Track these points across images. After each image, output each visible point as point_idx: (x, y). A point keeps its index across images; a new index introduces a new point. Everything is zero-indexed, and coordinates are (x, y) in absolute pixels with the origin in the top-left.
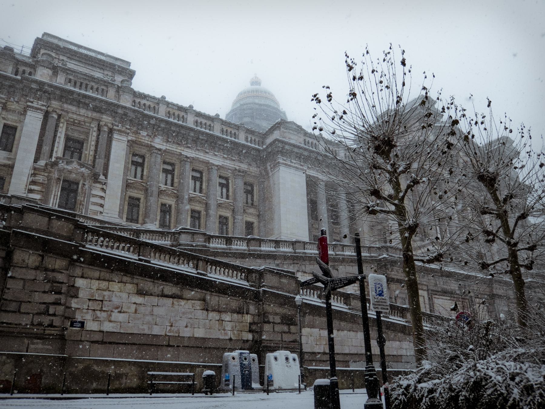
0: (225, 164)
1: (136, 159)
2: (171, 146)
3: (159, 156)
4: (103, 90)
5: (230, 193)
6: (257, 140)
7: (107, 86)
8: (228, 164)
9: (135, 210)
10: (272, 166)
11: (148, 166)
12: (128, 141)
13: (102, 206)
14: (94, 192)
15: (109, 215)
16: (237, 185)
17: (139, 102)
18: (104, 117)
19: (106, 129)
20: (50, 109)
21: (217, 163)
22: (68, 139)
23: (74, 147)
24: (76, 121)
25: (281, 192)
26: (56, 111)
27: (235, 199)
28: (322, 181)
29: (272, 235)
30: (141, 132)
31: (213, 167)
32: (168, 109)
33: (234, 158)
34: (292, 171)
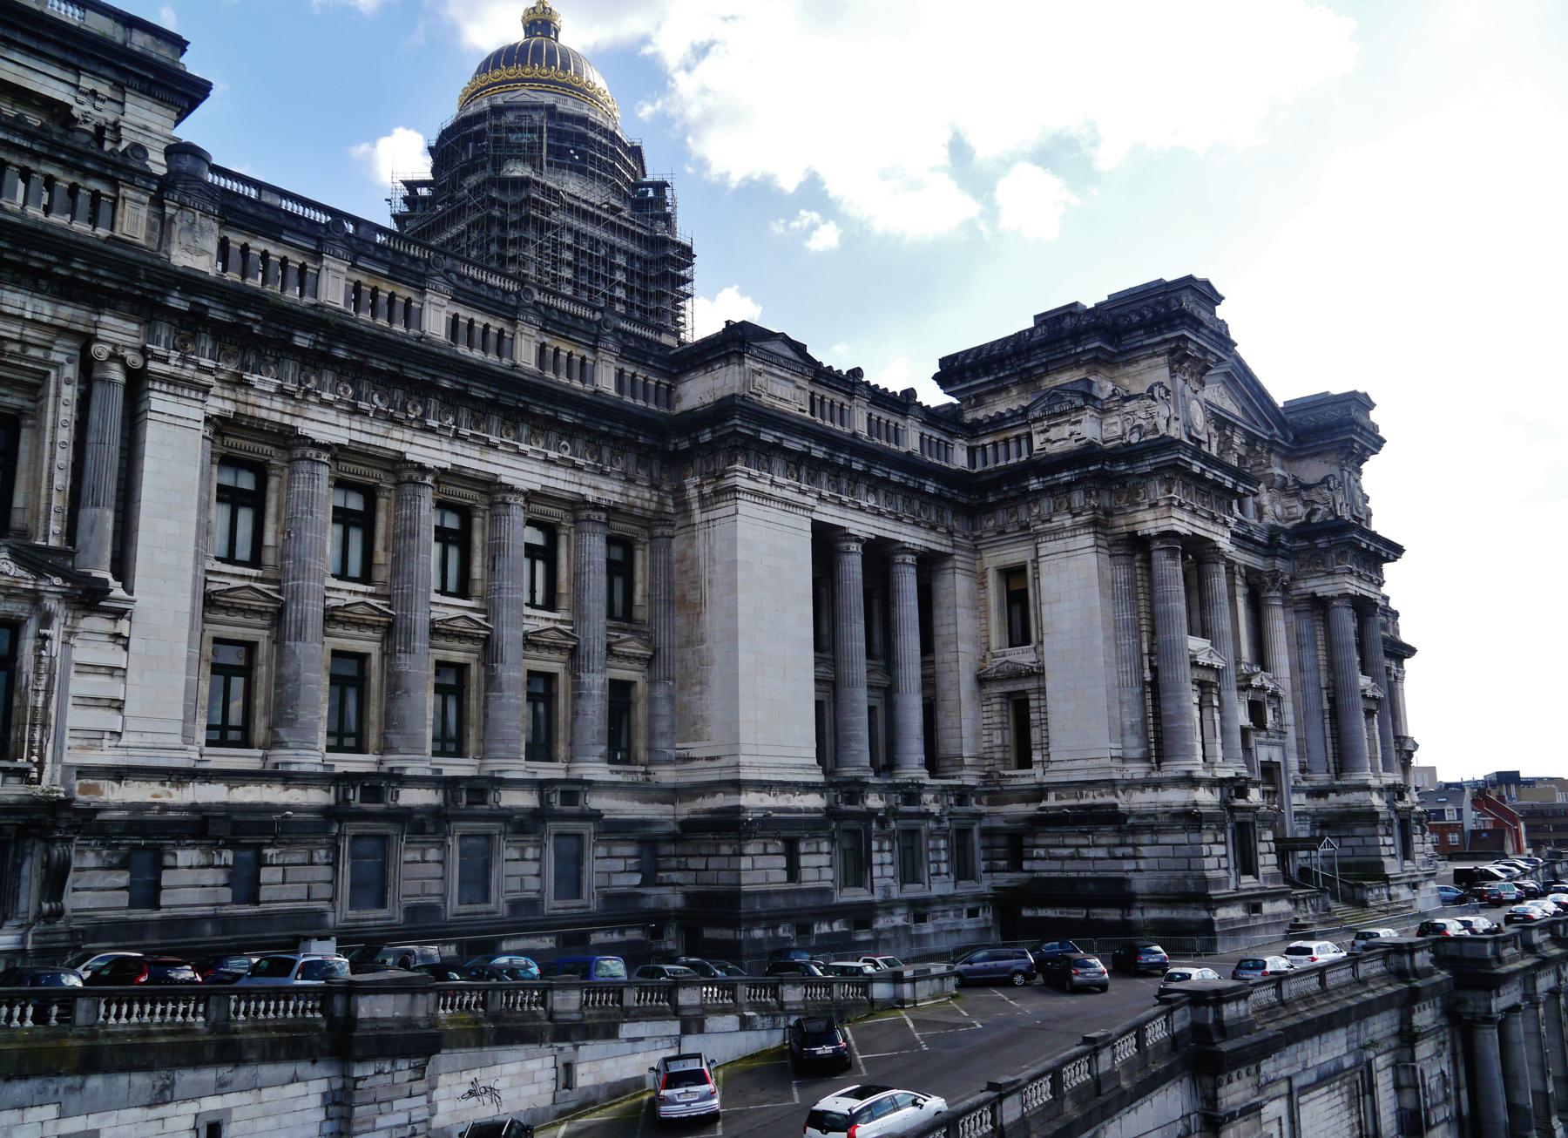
0: (551, 483)
1: (228, 479)
2: (367, 428)
4: (96, 195)
6: (652, 380)
7: (114, 183)
8: (561, 481)
9: (237, 684)
10: (707, 490)
11: (279, 507)
12: (208, 420)
13: (118, 705)
15: (148, 740)
17: (245, 249)
18: (107, 319)
19: (116, 374)
25: (741, 597)
27: (578, 606)
29: (698, 737)
30: (256, 377)
31: (511, 498)
32: (356, 277)
33: (580, 461)
34: (774, 513)
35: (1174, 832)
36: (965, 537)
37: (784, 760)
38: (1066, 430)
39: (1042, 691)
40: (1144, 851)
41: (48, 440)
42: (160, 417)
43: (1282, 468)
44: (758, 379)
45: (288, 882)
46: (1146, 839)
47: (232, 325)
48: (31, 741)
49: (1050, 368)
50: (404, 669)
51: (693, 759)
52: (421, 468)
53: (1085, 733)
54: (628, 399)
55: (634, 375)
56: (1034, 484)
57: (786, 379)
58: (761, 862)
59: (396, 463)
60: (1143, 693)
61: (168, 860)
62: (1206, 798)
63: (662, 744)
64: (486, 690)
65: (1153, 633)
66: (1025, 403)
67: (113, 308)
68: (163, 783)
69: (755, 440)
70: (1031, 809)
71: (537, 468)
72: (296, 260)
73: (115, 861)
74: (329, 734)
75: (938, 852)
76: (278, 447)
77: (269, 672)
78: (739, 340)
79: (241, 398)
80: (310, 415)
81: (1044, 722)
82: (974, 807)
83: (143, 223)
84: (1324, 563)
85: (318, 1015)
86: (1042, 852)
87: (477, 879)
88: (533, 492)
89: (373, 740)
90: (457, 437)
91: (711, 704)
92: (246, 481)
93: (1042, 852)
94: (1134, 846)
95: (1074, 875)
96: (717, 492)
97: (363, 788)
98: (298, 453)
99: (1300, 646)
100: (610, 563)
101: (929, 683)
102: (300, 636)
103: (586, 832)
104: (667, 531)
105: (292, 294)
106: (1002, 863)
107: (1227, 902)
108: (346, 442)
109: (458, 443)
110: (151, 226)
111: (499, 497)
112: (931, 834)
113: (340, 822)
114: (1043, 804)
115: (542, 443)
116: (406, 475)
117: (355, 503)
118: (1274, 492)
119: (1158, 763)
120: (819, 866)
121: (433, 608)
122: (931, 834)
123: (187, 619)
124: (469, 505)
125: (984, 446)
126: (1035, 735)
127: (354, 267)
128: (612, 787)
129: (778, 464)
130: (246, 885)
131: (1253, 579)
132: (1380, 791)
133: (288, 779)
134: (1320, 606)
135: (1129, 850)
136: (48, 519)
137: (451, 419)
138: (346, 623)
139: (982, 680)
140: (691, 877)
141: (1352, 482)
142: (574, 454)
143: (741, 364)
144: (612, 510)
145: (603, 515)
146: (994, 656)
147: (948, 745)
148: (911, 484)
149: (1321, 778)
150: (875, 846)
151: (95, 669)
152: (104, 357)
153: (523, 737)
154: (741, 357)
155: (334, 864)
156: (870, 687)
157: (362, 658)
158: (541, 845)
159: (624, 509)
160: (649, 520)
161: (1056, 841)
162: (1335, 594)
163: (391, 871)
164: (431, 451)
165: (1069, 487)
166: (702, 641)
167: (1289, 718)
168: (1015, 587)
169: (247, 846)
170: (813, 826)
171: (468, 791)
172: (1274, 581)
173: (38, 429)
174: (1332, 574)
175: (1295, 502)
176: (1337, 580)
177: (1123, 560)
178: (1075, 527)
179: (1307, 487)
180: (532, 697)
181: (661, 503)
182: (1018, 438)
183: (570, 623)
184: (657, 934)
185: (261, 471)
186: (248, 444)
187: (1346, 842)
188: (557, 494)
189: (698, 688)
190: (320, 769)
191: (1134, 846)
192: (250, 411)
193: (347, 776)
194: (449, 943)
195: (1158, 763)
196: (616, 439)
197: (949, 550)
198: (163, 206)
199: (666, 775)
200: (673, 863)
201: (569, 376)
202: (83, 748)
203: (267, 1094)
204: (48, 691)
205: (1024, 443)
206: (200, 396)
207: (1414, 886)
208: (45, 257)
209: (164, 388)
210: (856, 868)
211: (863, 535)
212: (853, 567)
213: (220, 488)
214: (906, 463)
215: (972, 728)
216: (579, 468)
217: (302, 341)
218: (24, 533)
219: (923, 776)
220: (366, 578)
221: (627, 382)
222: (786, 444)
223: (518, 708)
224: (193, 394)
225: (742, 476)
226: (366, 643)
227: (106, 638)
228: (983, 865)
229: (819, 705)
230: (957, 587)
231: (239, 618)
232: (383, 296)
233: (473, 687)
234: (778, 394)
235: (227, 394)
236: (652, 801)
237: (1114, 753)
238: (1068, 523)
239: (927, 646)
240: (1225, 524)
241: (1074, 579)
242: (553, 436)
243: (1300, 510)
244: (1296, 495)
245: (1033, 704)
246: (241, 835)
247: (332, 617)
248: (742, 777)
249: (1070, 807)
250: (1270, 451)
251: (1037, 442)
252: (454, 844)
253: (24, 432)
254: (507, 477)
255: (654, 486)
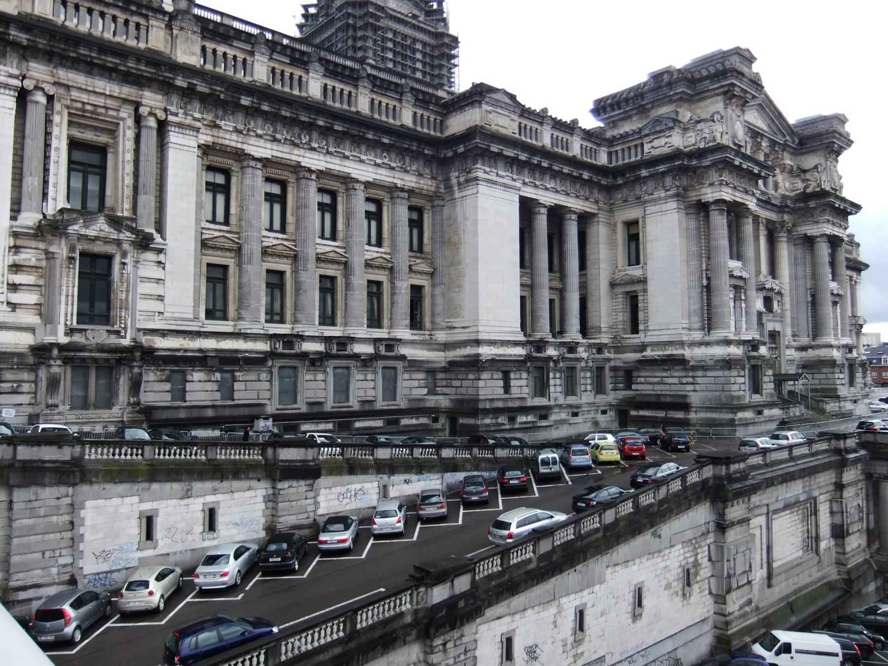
0: (378, 177)
2: (280, 149)
3: (259, 173)
5: (386, 234)
6: (432, 117)
7: (146, 17)
8: (384, 176)
9: (219, 287)
10: (462, 179)
11: (237, 193)
12: (199, 147)
14: (143, 272)
16: (398, 215)
17: (214, 51)
19: (152, 123)
20: (29, 84)
21: (363, 179)
22: (74, 144)
23: (90, 159)
24: (88, 107)
25: (481, 239)
26: (43, 89)
27: (393, 245)
28: (545, 206)
29: (457, 316)
30: (223, 122)
32: (272, 64)
34: (498, 192)
35: (717, 370)
36: (605, 204)
37: (503, 329)
38: (663, 141)
39: (645, 291)
40: (699, 380)
41: (121, 160)
42: (175, 146)
43: (791, 160)
44: (490, 116)
45: (251, 389)
46: (700, 373)
47: (209, 95)
48: (120, 317)
49: (655, 104)
50: (303, 279)
51: (454, 328)
52: (309, 170)
53: (669, 314)
54: (419, 129)
55: (422, 115)
56: (644, 173)
57: (505, 115)
58: (490, 383)
59: (297, 169)
60: (702, 292)
61: (189, 378)
62: (736, 351)
63: (438, 319)
64: (346, 290)
65: (709, 258)
66: (640, 126)
67: (149, 87)
68: (185, 338)
69: (488, 150)
70: (637, 356)
71: (371, 169)
72: (241, 56)
73: (164, 378)
74: (266, 314)
75: (585, 379)
76: (236, 160)
77: (235, 281)
78: (480, 93)
79: (215, 134)
80: (251, 142)
81: (646, 308)
82: (606, 355)
83: (162, 39)
84: (812, 216)
85: (260, 457)
86: (642, 380)
87: (343, 389)
88: (368, 182)
89: (288, 316)
90: (328, 153)
91: (465, 298)
92: (220, 179)
93: (642, 380)
94: (693, 377)
95: (659, 392)
96: (467, 181)
97: (283, 342)
98: (245, 164)
99: (796, 264)
100: (410, 220)
101: (583, 286)
102: (250, 262)
103: (398, 366)
104: (441, 203)
105: (240, 75)
106: (621, 385)
107: (743, 408)
108: (270, 157)
109: (328, 156)
110: (166, 40)
111: (351, 186)
112: (583, 369)
113: (273, 360)
114: (644, 354)
115: (373, 155)
116: (301, 175)
117: (276, 190)
118: (786, 175)
119: (709, 332)
120: (521, 385)
121: (317, 246)
122: (583, 369)
123: (193, 252)
124: (335, 189)
125: (617, 151)
126: (641, 316)
127: (271, 59)
128: (412, 343)
129: (501, 164)
130: (227, 390)
131: (770, 226)
132: (838, 347)
133: (246, 336)
134: (809, 241)
135: (690, 380)
136: (123, 202)
137: (324, 143)
138: (273, 255)
139: (613, 285)
140: (453, 390)
141: (832, 167)
142: (390, 160)
143: (480, 107)
144: (411, 192)
145: (406, 195)
146: (620, 271)
147: (592, 321)
148: (574, 174)
149: (805, 340)
150: (551, 375)
151: (149, 279)
152: (146, 114)
153: (366, 315)
154: (480, 102)
155: (270, 381)
156: (551, 288)
157: (281, 274)
158: (375, 373)
159: (417, 191)
160: (431, 197)
161: (650, 374)
162: (818, 234)
163: (299, 385)
164: (314, 161)
165: (664, 174)
166: (459, 264)
167: (788, 306)
168: (633, 232)
169: (227, 371)
170: (520, 364)
171: (337, 344)
172: (783, 226)
173: (116, 154)
174: (817, 222)
175: (798, 180)
176: (820, 226)
177: (693, 216)
178: (666, 198)
179: (805, 172)
180: (370, 294)
181: (438, 187)
182: (636, 146)
183: (390, 254)
184: (435, 420)
185: (227, 173)
186: (220, 159)
187: (816, 376)
188: (382, 183)
189: (457, 289)
190: (262, 332)
191: (693, 377)
192: (220, 141)
193: (275, 336)
194: (329, 422)
195: (709, 332)
196: (412, 151)
197: (596, 212)
198: (171, 29)
199: (441, 336)
200: (444, 383)
201: (387, 116)
202: (145, 320)
203: (236, 495)
204: (127, 291)
205: (639, 149)
206: (195, 133)
207: (855, 402)
208: (114, 60)
209: (177, 130)
210: (542, 388)
211: (547, 204)
212: (542, 222)
213: (208, 183)
214: (573, 162)
215: (607, 312)
216: (393, 169)
217: (245, 101)
218: (113, 209)
219: (579, 338)
220: (283, 230)
221: (419, 119)
222: (505, 153)
223: (363, 300)
224: (191, 133)
225: (481, 171)
226: (284, 266)
227: (153, 264)
228: (610, 386)
229: (523, 298)
230: (600, 232)
231: (219, 253)
232: (287, 75)
233: (339, 289)
234: (501, 124)
235: (208, 132)
236: (433, 350)
237: (684, 326)
238: (663, 195)
239: (583, 266)
240: (753, 194)
241: (666, 228)
242: (379, 151)
243: (800, 185)
244: (798, 176)
245: (640, 298)
246: (227, 363)
247: (265, 252)
248: (480, 338)
249: (659, 356)
250: (783, 150)
251: (646, 150)
252: (330, 370)
253: (110, 157)
254: (355, 174)
255: (433, 178)
